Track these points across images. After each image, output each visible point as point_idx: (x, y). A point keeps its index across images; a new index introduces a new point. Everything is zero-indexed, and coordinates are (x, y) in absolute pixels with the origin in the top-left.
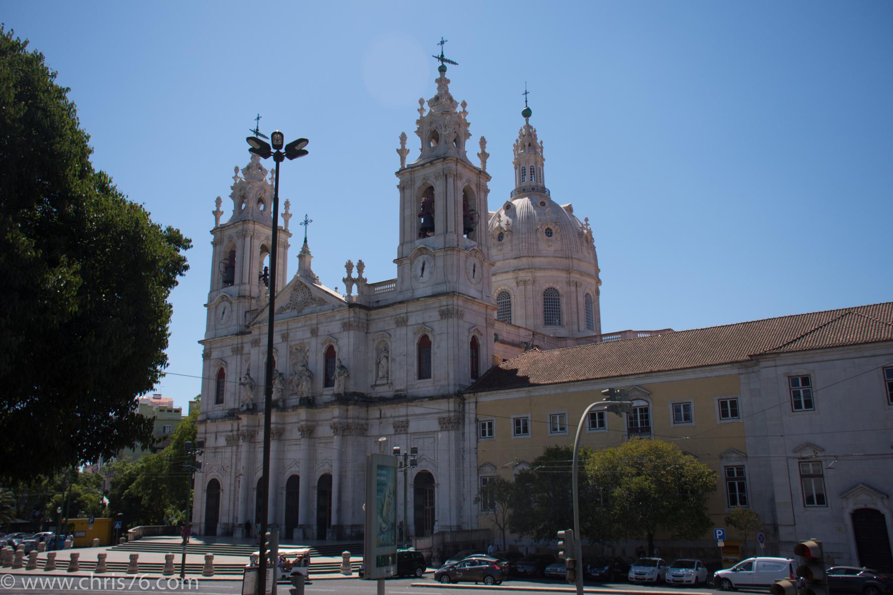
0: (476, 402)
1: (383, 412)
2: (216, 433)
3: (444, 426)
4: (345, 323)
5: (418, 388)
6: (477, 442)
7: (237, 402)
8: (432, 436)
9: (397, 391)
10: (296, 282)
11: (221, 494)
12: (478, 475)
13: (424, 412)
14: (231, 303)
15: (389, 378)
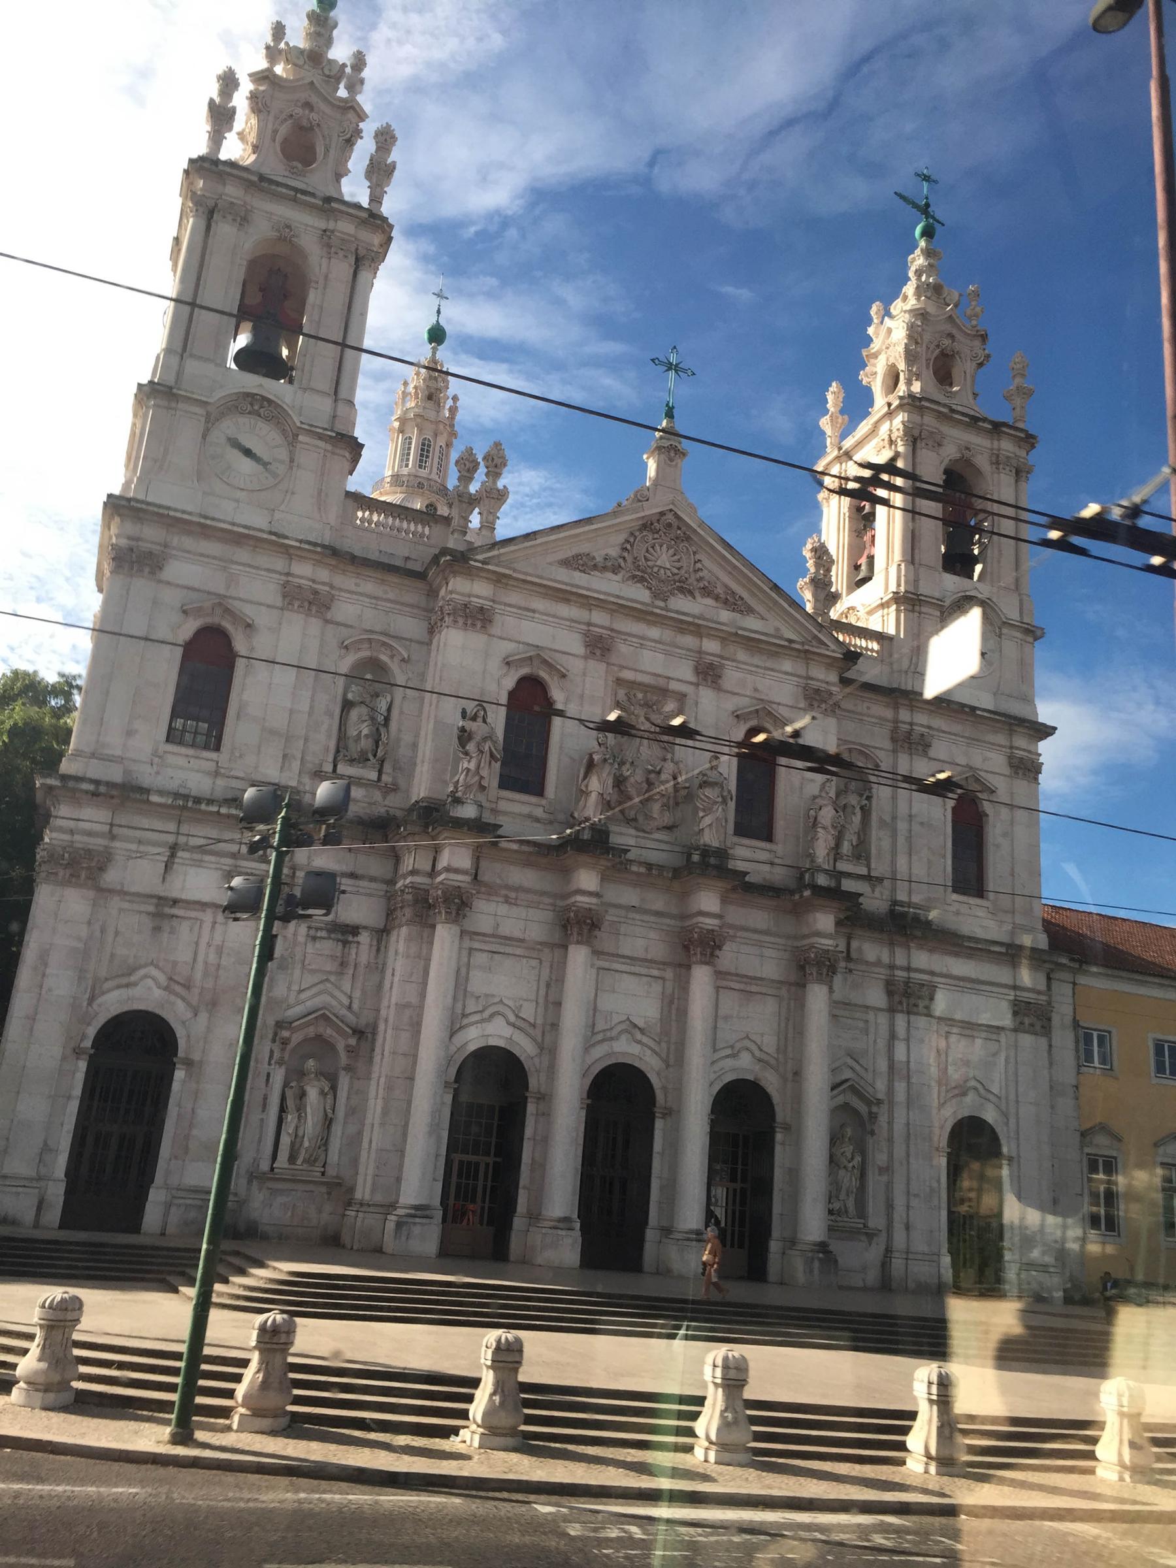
0: (1074, 984)
1: (855, 944)
2: (174, 849)
3: (1027, 1021)
4: (817, 691)
5: (958, 913)
6: (1079, 1073)
7: (296, 765)
8: (994, 1037)
9: (895, 903)
10: (662, 514)
11: (179, 1074)
12: (1082, 1148)
13: (973, 976)
14: (291, 436)
15: (873, 866)
